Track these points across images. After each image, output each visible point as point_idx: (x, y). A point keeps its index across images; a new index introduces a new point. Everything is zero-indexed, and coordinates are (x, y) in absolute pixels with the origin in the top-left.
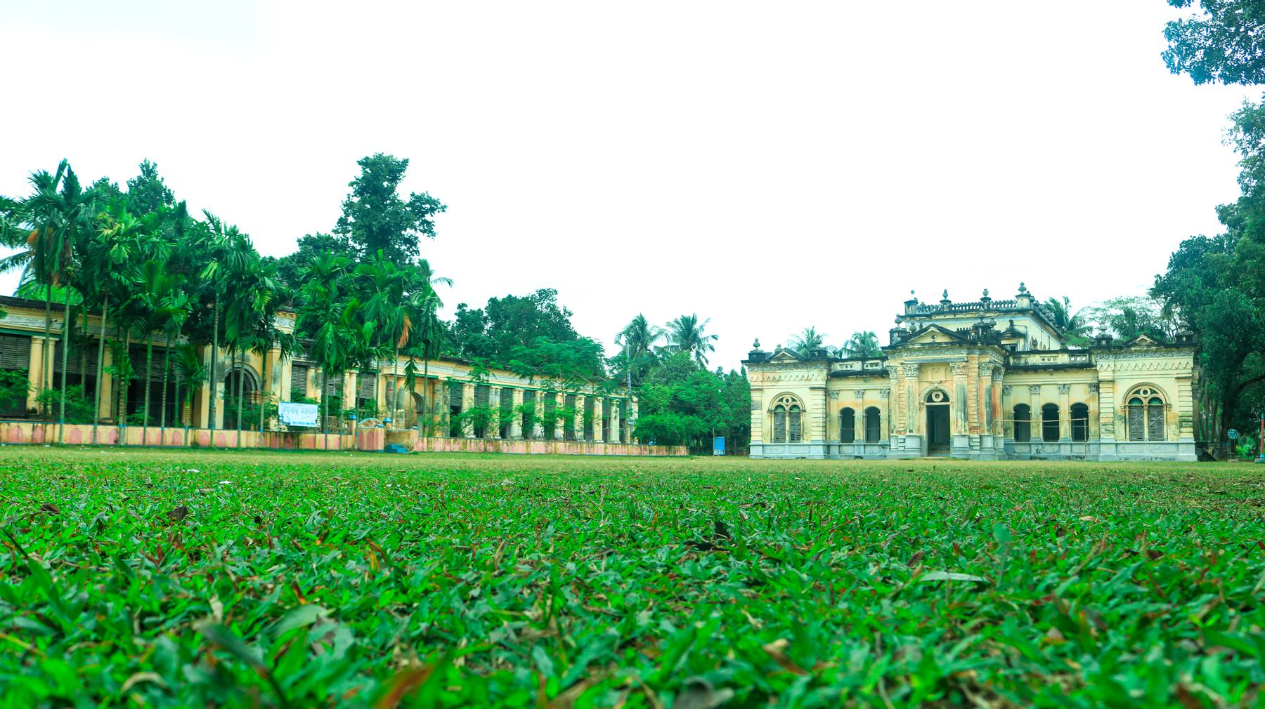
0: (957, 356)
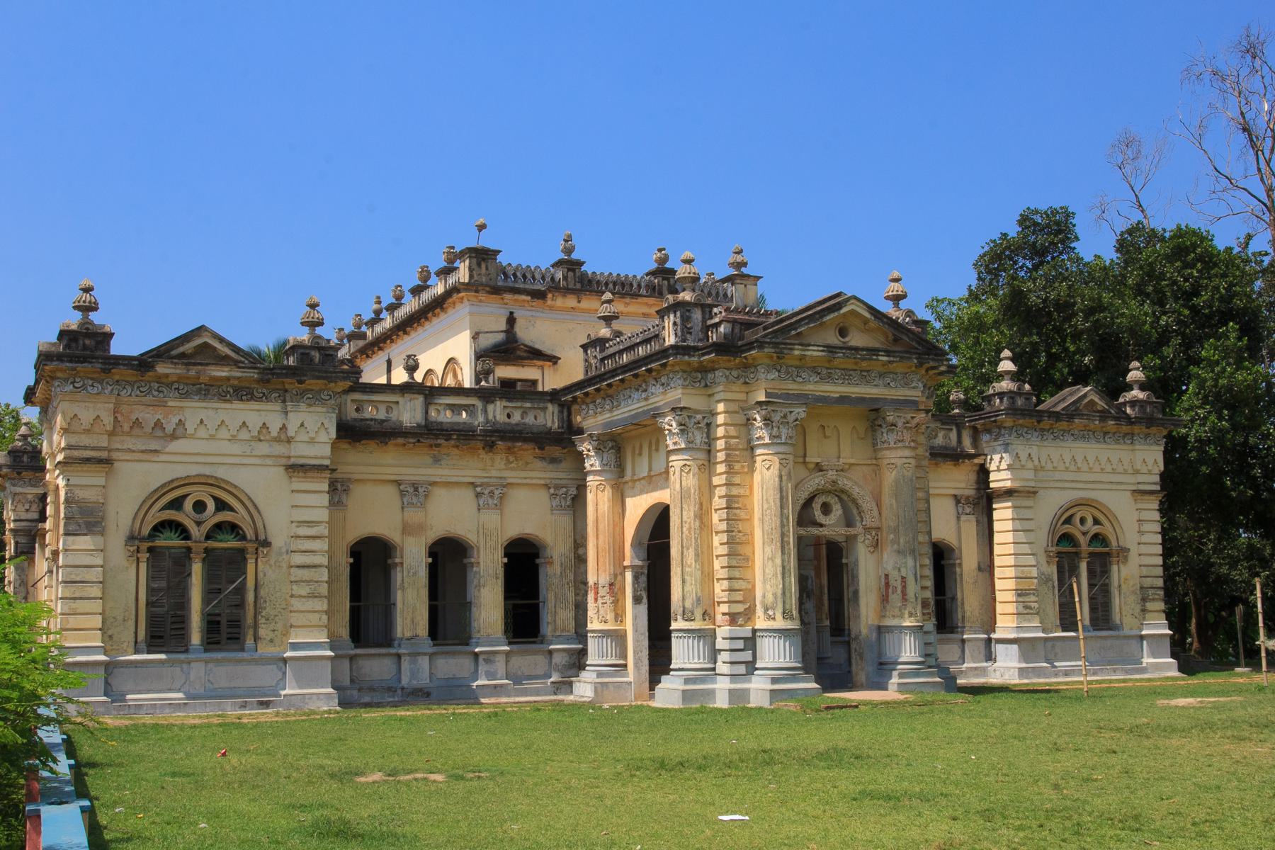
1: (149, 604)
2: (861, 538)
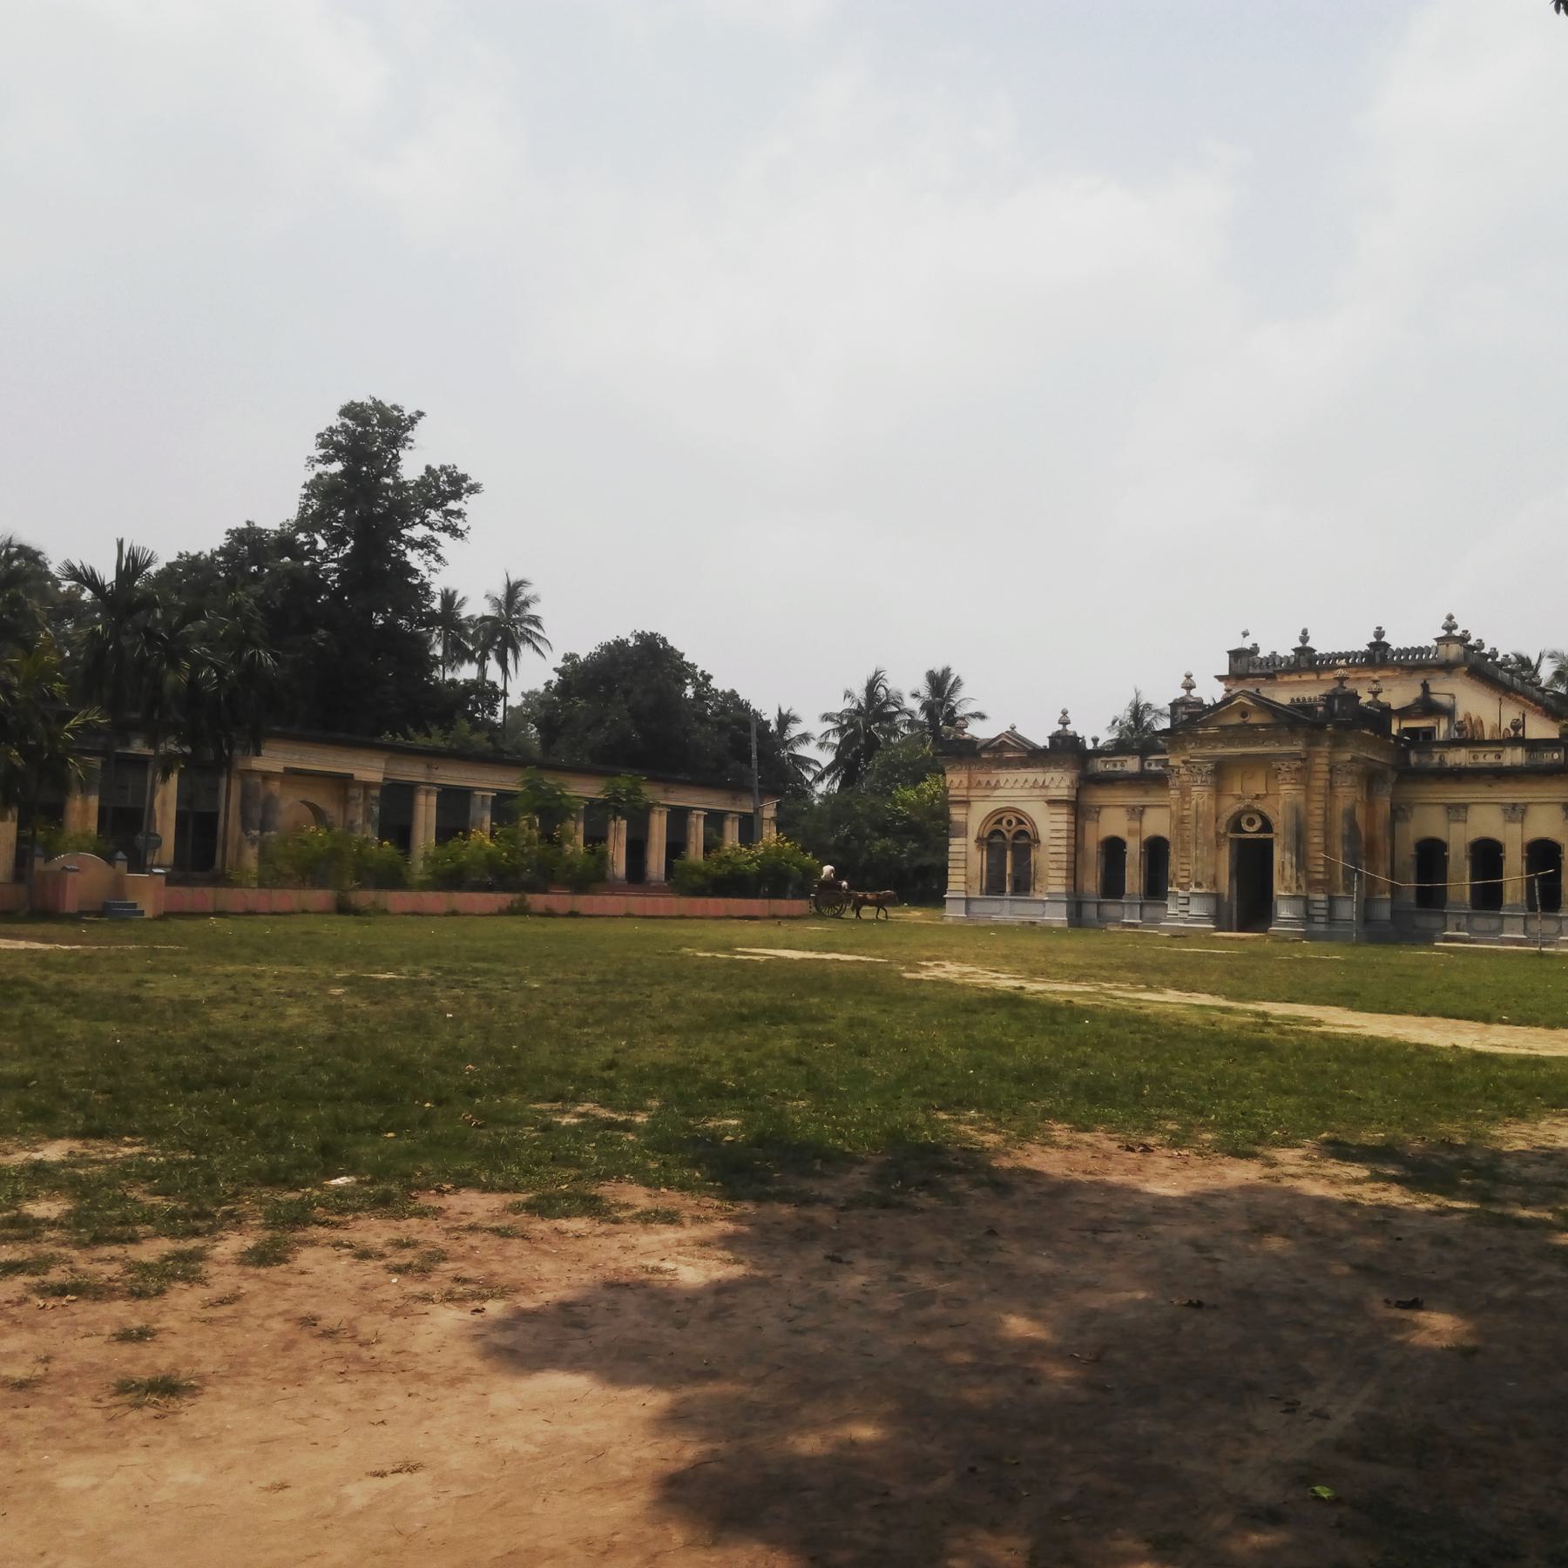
0: (1286, 749)
1: (988, 871)
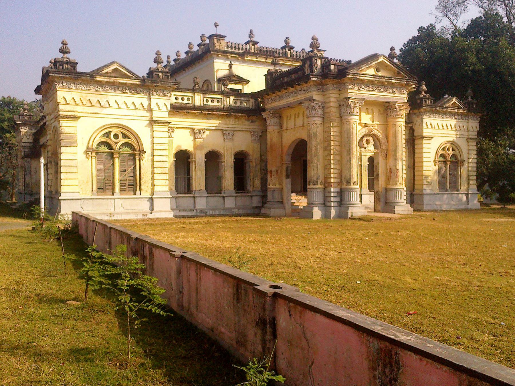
2: (380, 154)
